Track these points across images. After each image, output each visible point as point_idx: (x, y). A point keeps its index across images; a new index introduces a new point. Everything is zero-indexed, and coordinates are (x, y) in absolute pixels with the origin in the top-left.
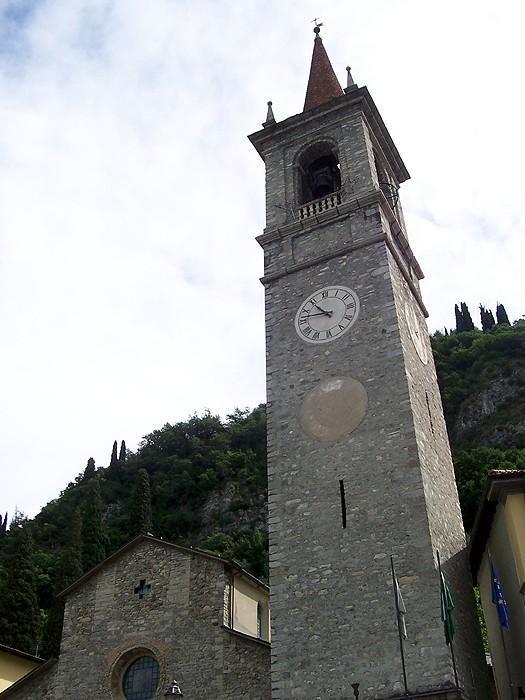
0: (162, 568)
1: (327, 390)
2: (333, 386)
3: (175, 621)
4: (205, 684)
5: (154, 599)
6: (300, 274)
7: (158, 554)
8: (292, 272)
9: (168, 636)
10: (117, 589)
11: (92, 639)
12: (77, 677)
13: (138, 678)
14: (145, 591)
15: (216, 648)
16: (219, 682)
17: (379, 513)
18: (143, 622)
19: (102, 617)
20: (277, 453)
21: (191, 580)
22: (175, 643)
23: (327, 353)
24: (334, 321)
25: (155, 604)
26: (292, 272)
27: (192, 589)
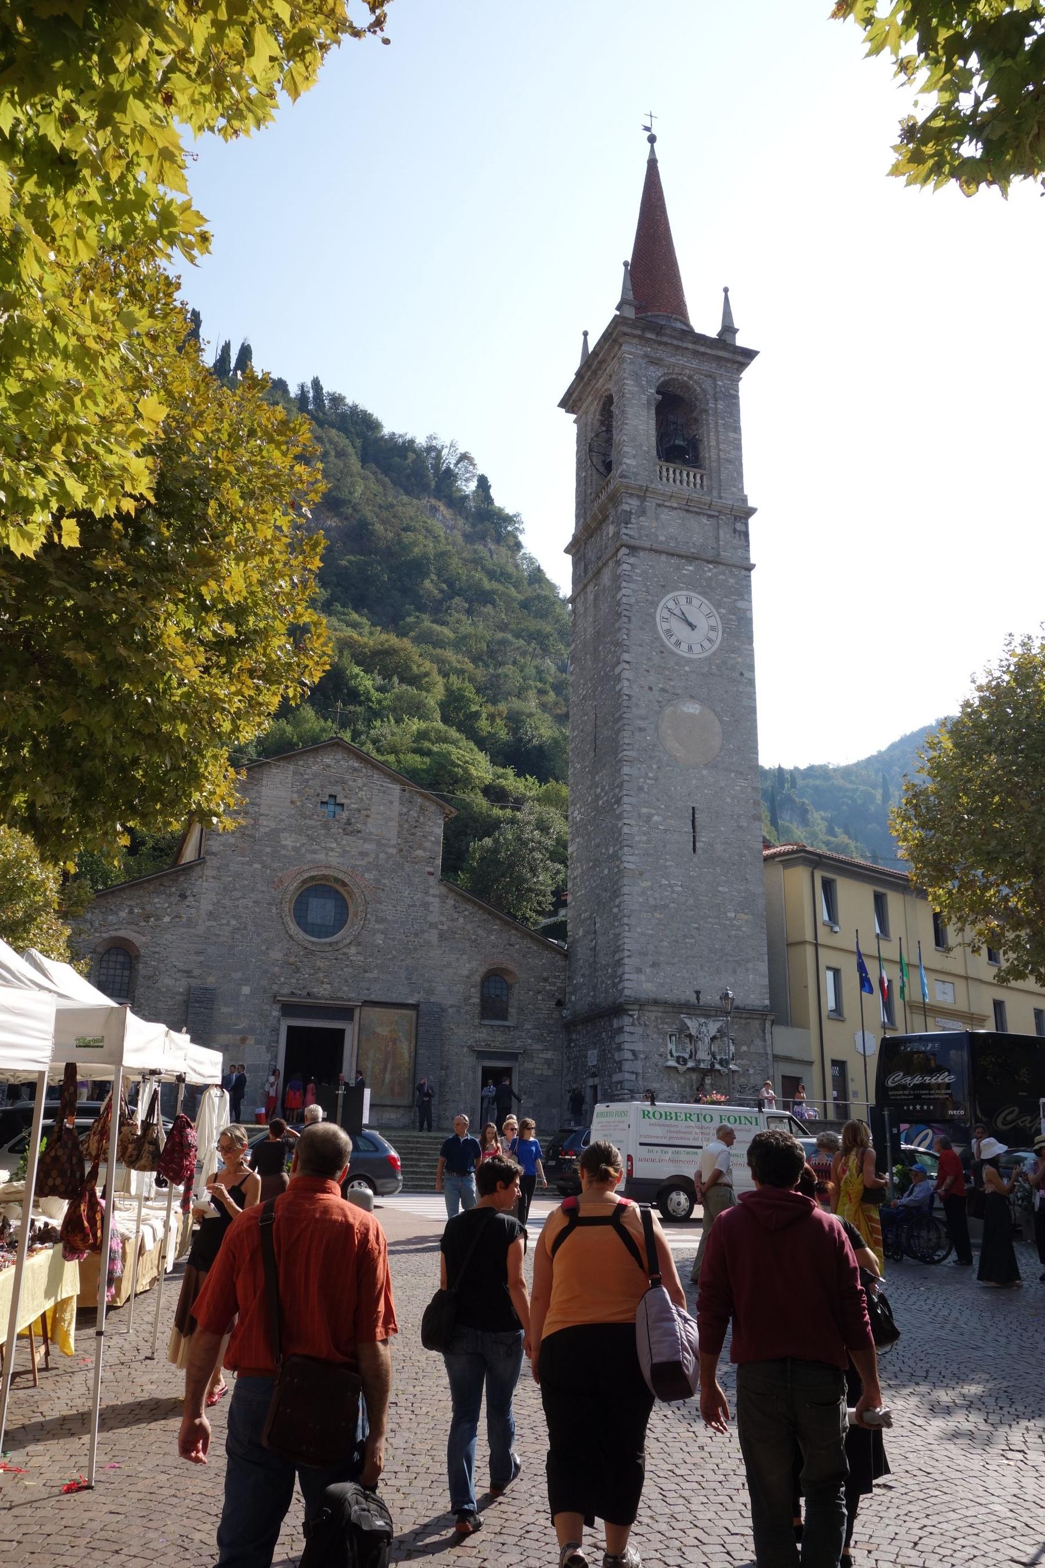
0: (361, 789)
1: (685, 709)
2: (692, 708)
3: (377, 856)
4: (416, 935)
5: (349, 823)
6: (664, 558)
7: (355, 770)
8: (656, 551)
9: (369, 870)
10: (295, 796)
11: (257, 848)
12: (235, 889)
13: (321, 910)
14: (331, 808)
15: (430, 899)
16: (433, 936)
17: (725, 850)
18: (334, 845)
19: (273, 825)
20: (633, 754)
21: (401, 814)
22: (377, 881)
23: (687, 669)
24: (696, 637)
25: (349, 829)
26: (656, 551)
27: (400, 826)
